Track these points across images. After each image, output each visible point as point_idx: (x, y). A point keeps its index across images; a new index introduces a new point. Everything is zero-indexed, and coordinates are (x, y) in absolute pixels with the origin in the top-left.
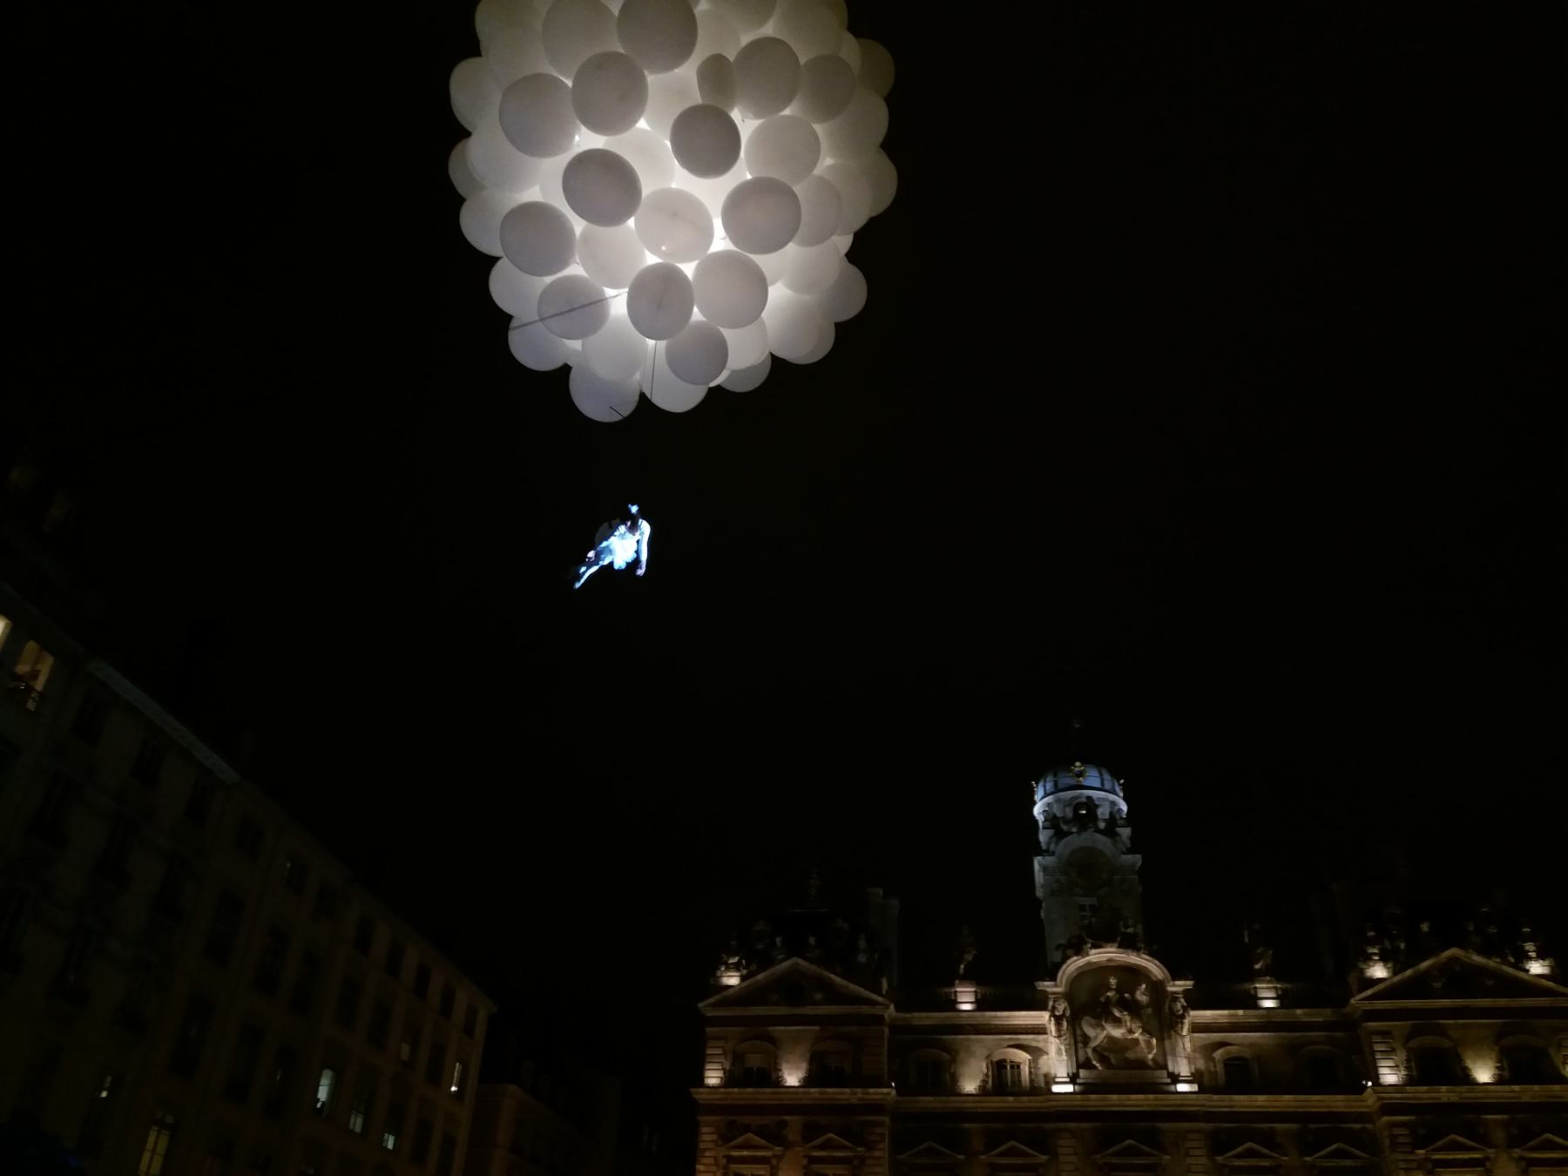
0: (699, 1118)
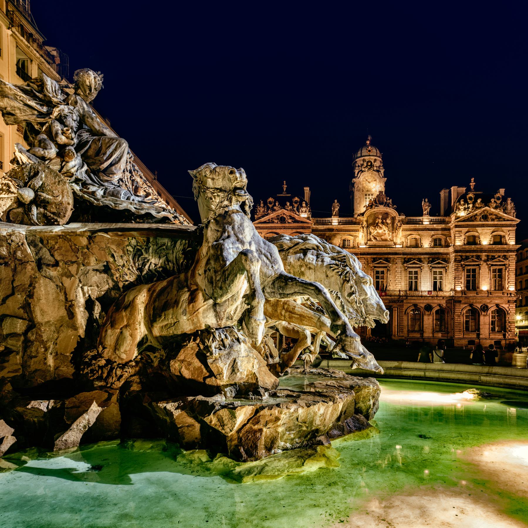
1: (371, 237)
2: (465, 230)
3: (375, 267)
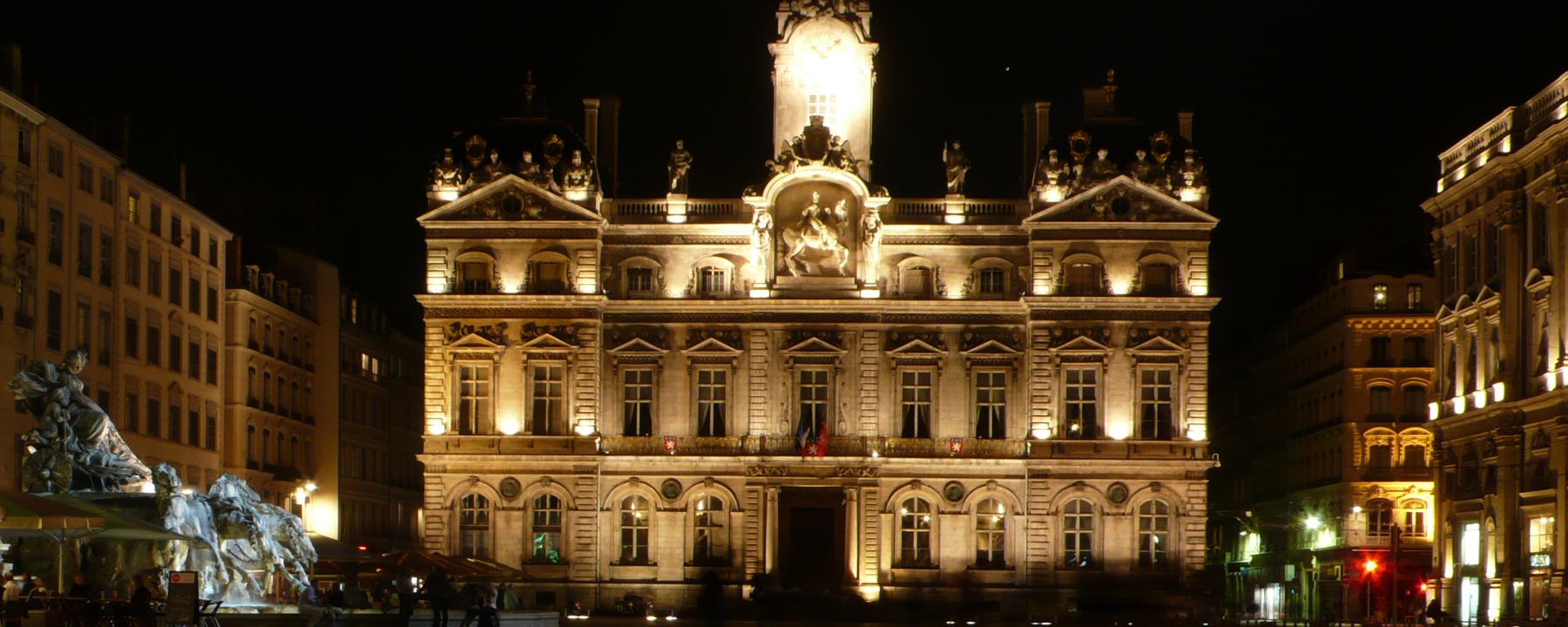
0: (424, 320)
1: (788, 260)
2: (1062, 245)
3: (797, 360)
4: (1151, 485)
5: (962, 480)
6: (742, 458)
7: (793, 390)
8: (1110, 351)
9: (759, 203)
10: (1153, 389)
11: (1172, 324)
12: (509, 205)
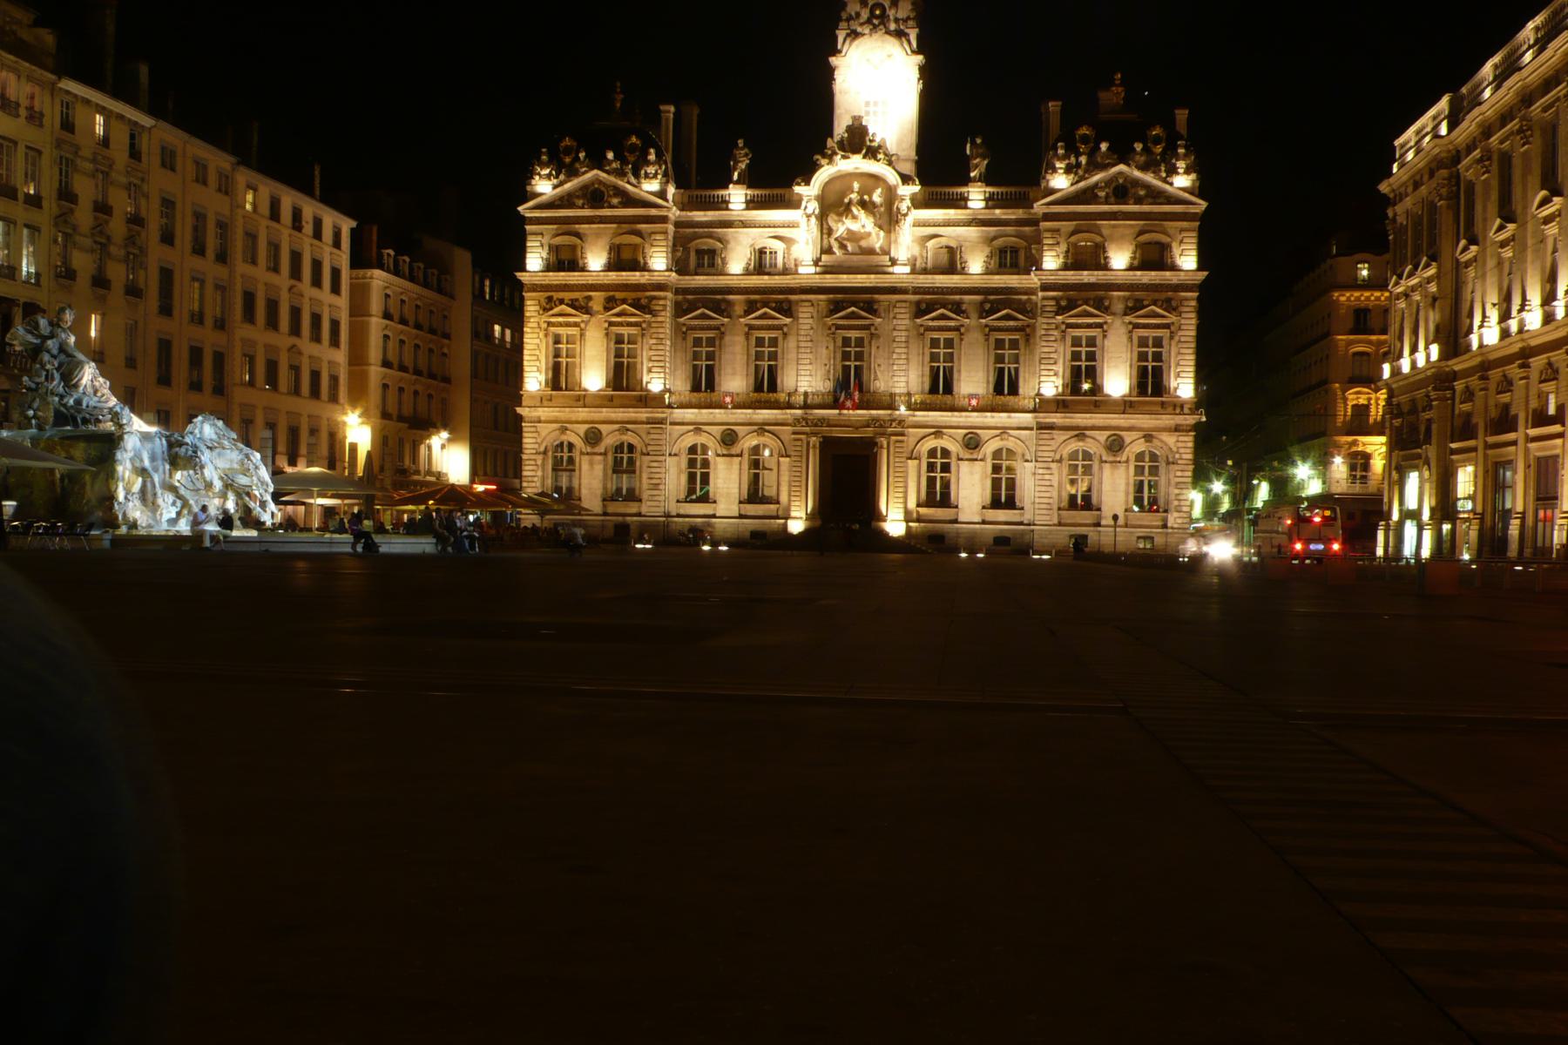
0: (524, 294)
1: (832, 241)
3: (838, 327)
4: (1144, 437)
5: (978, 431)
6: (788, 411)
7: (835, 352)
8: (1109, 319)
9: (808, 192)
10: (1147, 352)
11: (1163, 296)
12: (594, 196)
